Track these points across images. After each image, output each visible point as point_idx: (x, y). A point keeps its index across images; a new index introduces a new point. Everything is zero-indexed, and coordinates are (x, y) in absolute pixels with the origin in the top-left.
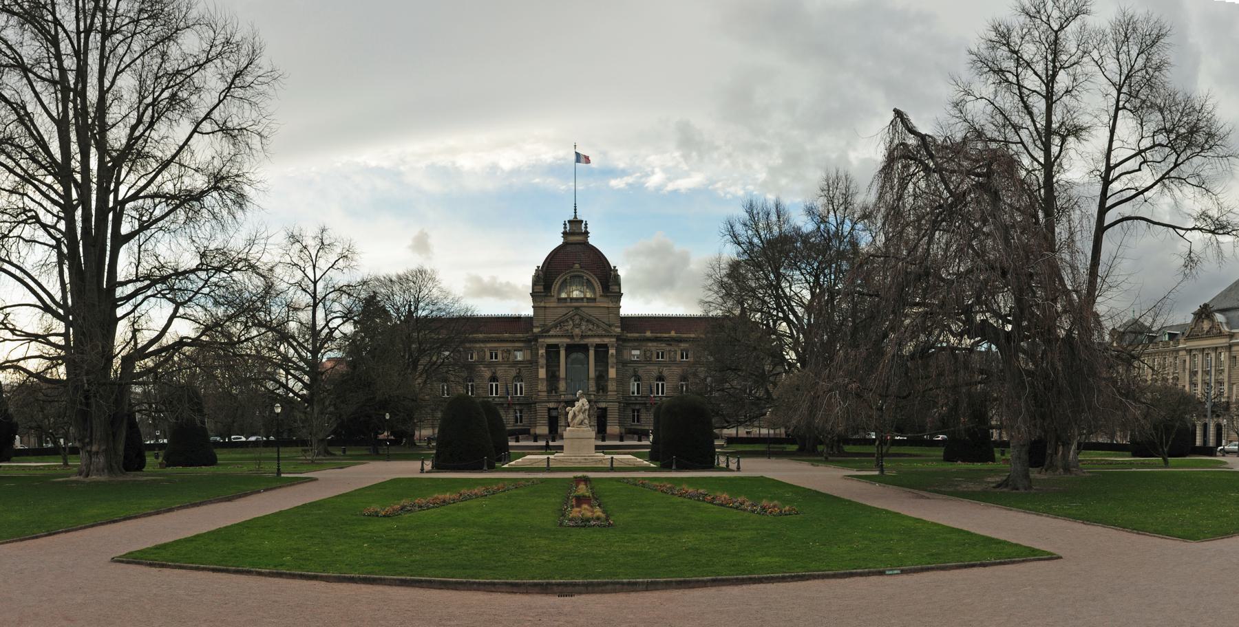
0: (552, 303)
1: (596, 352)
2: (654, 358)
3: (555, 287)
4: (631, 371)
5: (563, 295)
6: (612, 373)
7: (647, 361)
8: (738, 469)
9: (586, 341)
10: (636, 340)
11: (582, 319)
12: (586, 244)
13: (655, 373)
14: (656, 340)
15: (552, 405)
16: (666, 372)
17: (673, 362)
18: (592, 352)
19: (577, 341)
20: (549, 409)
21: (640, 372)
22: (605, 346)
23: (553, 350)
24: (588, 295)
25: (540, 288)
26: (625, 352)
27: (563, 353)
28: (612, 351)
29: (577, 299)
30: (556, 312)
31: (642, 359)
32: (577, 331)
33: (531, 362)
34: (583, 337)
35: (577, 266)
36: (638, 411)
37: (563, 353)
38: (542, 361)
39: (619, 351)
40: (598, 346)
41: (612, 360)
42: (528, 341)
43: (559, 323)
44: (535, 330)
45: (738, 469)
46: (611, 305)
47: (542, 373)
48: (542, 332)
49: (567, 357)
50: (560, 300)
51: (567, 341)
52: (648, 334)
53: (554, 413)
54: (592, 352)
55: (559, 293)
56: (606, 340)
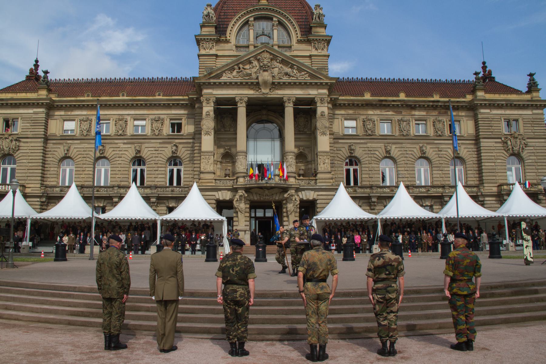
4: (345, 152)
6: (324, 143)
9: (279, 93)
11: (274, 58)
13: (381, 152)
18: (289, 111)
19: (266, 92)
21: (359, 152)
22: (311, 102)
27: (242, 112)
28: (322, 109)
31: (361, 132)
32: (266, 76)
34: (275, 85)
37: (242, 112)
38: (208, 124)
41: (321, 123)
46: (314, 52)
49: (248, 126)
51: (250, 93)
52: (368, 96)
54: (289, 111)
56: (312, 92)
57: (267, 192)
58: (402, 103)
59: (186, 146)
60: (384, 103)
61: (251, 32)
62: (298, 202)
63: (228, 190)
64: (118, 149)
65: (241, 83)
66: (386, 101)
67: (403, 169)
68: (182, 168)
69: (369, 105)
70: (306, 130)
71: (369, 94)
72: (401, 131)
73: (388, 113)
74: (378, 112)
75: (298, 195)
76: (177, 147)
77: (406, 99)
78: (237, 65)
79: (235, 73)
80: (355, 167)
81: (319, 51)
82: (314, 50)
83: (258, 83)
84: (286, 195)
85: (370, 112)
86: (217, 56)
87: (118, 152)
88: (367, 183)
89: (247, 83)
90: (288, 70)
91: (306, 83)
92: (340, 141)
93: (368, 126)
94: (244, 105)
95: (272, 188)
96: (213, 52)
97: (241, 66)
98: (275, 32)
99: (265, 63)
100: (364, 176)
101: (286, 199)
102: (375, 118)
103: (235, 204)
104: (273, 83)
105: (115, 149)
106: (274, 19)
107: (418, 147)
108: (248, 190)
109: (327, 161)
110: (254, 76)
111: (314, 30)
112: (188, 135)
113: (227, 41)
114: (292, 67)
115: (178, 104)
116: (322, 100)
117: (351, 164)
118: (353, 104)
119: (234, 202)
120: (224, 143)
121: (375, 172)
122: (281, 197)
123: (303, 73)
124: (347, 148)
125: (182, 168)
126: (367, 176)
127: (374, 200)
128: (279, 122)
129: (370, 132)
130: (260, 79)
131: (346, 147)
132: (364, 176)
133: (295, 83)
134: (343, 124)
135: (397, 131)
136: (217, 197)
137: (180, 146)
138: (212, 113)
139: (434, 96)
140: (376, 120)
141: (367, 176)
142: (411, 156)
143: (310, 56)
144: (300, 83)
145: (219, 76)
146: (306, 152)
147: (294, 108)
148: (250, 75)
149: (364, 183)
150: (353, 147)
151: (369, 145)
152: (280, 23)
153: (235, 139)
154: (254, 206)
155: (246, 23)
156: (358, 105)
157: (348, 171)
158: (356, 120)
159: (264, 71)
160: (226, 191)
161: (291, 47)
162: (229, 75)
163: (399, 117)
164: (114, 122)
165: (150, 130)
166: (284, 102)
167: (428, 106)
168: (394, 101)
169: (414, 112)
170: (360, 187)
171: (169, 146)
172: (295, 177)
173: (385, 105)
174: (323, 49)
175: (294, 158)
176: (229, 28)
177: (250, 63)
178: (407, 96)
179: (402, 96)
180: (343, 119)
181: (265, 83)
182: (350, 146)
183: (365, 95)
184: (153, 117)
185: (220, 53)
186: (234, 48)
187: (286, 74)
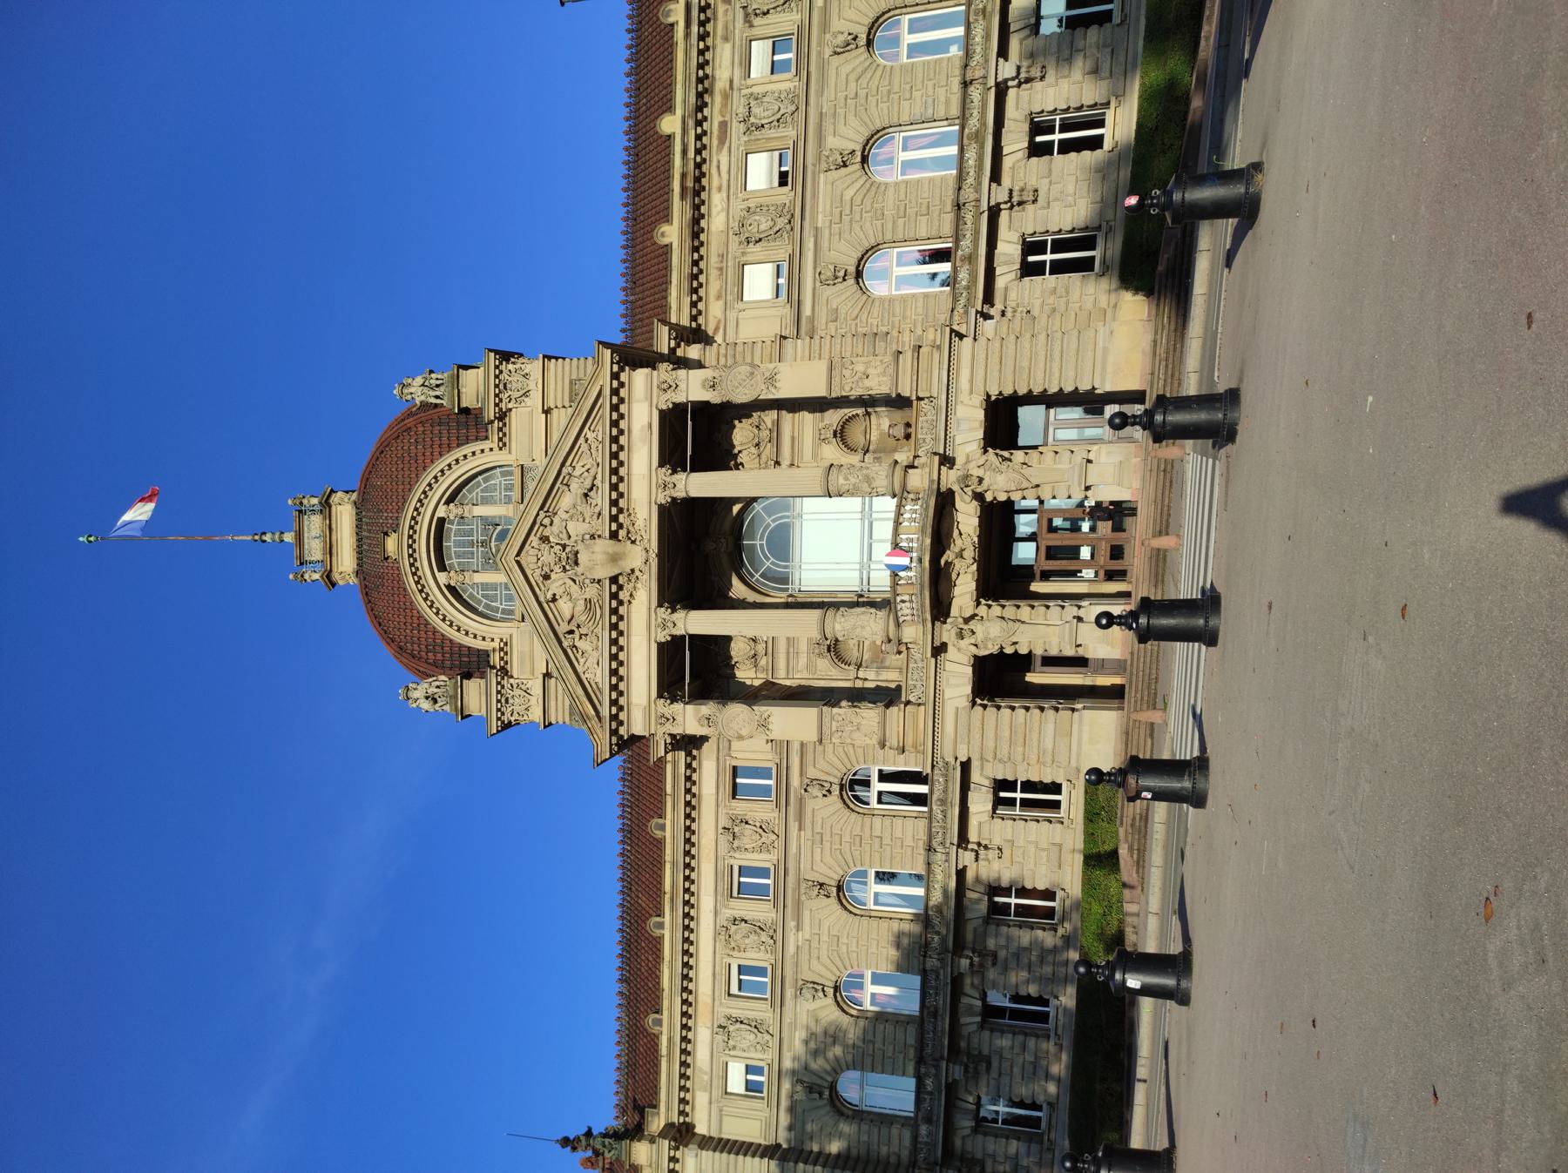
14: (696, 192)
19: (641, 555)
58: (691, 123)
60: (690, 184)
64: (815, 944)
66: (684, 176)
69: (696, 229)
71: (665, 228)
73: (724, 168)
77: (679, 112)
83: (614, 580)
85: (717, 222)
87: (824, 946)
93: (762, 227)
102: (738, 207)
104: (614, 535)
105: (815, 953)
109: (860, 368)
110: (592, 592)
129: (782, 222)
130: (604, 573)
139: (671, 20)
140: (744, 205)
147: (693, 470)
148: (588, 602)
160: (943, 675)
162: (592, 661)
163: (736, 129)
164: (735, 953)
165: (764, 856)
166: (674, 499)
168: (684, 152)
169: (721, 84)
173: (698, 180)
178: (670, 109)
179: (670, 124)
180: (741, 306)
181: (615, 558)
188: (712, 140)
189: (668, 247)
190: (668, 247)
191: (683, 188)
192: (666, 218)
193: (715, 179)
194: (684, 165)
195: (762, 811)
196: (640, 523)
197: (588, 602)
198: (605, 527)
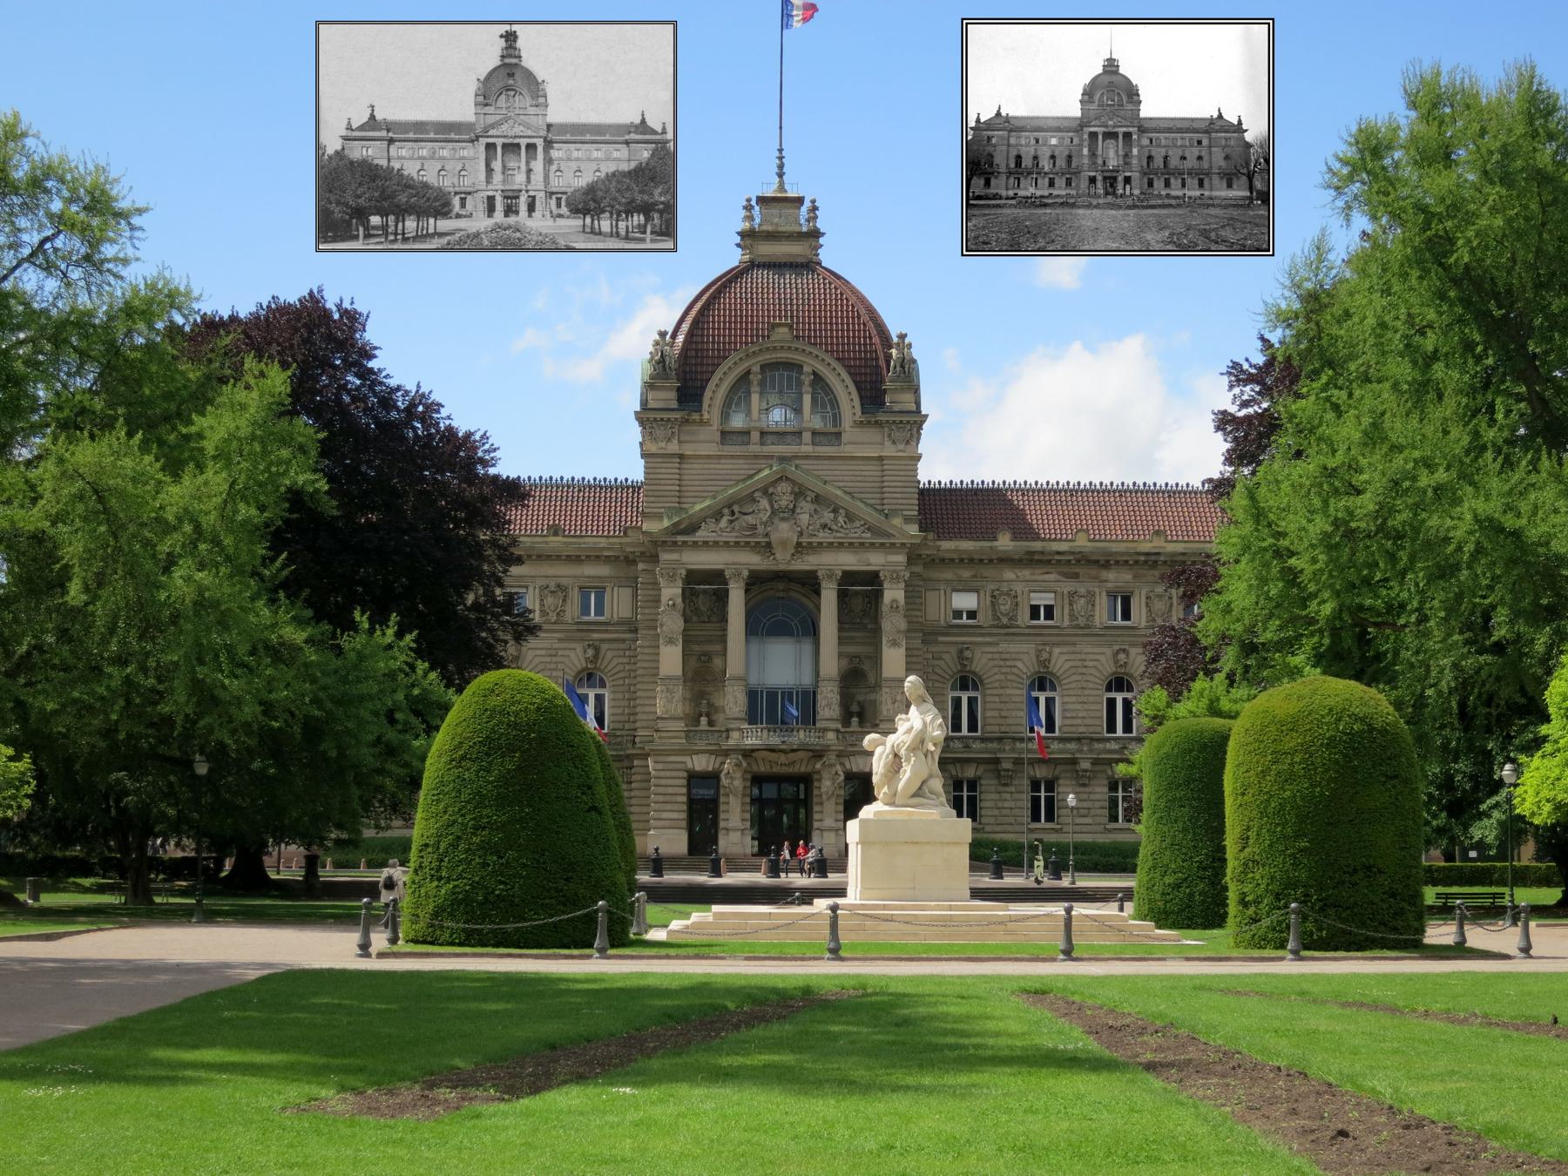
0: (703, 442)
1: (842, 596)
2: (1024, 617)
3: (715, 393)
5: (738, 422)
7: (1005, 627)
8: (1526, 950)
10: (970, 561)
12: (809, 265)
13: (1026, 666)
15: (701, 763)
16: (1060, 661)
17: (1085, 630)
19: (783, 560)
20: (694, 778)
21: (981, 662)
22: (873, 579)
23: (705, 593)
24: (817, 423)
25: (668, 397)
26: (932, 597)
28: (893, 594)
29: (781, 435)
30: (715, 473)
32: (784, 531)
33: (632, 626)
35: (783, 332)
36: (973, 785)
38: (673, 623)
39: (913, 594)
40: (849, 578)
41: (892, 623)
42: (630, 561)
43: (731, 508)
44: (650, 526)
45: (1526, 950)
46: (889, 450)
47: (671, 659)
48: (676, 530)
50: (726, 435)
51: (753, 560)
53: (703, 792)
55: (725, 415)
57: (783, 758)
59: (614, 646)
61: (755, 397)
62: (842, 778)
63: (711, 752)
65: (737, 543)
66: (1042, 553)
67: (1074, 699)
68: (606, 693)
70: (866, 621)
71: (1008, 536)
72: (1073, 617)
73: (1046, 577)
74: (1026, 573)
75: (842, 764)
76: (597, 650)
78: (730, 506)
79: (724, 523)
80: (972, 694)
81: (901, 447)
82: (888, 444)
84: (818, 766)
85: (1009, 575)
86: (681, 456)
88: (996, 729)
89: (747, 543)
90: (827, 516)
91: (862, 544)
92: (941, 639)
94: (742, 584)
95: (793, 751)
96: (673, 447)
97: (736, 508)
98: (807, 399)
99: (783, 503)
100: (989, 714)
101: (818, 772)
102: (1018, 588)
103: (724, 781)
106: (806, 369)
107: (1108, 651)
108: (748, 753)
110: (761, 529)
111: (887, 399)
112: (618, 623)
113: (702, 423)
114: (835, 511)
115: (597, 557)
116: (896, 578)
117: (964, 687)
118: (971, 560)
119: (722, 776)
120: (696, 648)
121: (1012, 706)
122: (809, 769)
123: (857, 524)
124: (954, 654)
125: (606, 693)
126: (996, 714)
127: (1005, 765)
128: (811, 606)
129: (1005, 621)
130: (774, 537)
131: (953, 650)
132: (989, 714)
133: (841, 544)
134: (948, 601)
135: (1066, 617)
136: (690, 766)
137: (604, 646)
138: (679, 600)
141: (996, 714)
142: (1093, 671)
143: (881, 458)
144: (851, 544)
145: (693, 528)
146: (866, 667)
149: (988, 728)
150: (968, 654)
151: (1003, 647)
152: (817, 379)
153: (723, 640)
154: (758, 780)
155: (745, 377)
156: (981, 560)
157: (957, 703)
158: (977, 591)
159: (783, 519)
161: (839, 435)
167: (1136, 562)
169: (1105, 574)
170: (983, 740)
171: (579, 647)
172: (838, 731)
173: (1039, 561)
174: (908, 443)
175: (836, 690)
176: (708, 394)
177: (754, 500)
181: (784, 543)
182: (961, 651)
183: (1000, 537)
184: (544, 582)
185: (688, 450)
186: (717, 437)
187: (824, 526)
188: (1066, 569)
189: (995, 539)
190: (995, 539)
191: (1033, 553)
192: (1014, 539)
193: (1038, 574)
194: (1050, 553)
195: (572, 611)
196: (806, 558)
197: (754, 527)
198: (804, 540)
